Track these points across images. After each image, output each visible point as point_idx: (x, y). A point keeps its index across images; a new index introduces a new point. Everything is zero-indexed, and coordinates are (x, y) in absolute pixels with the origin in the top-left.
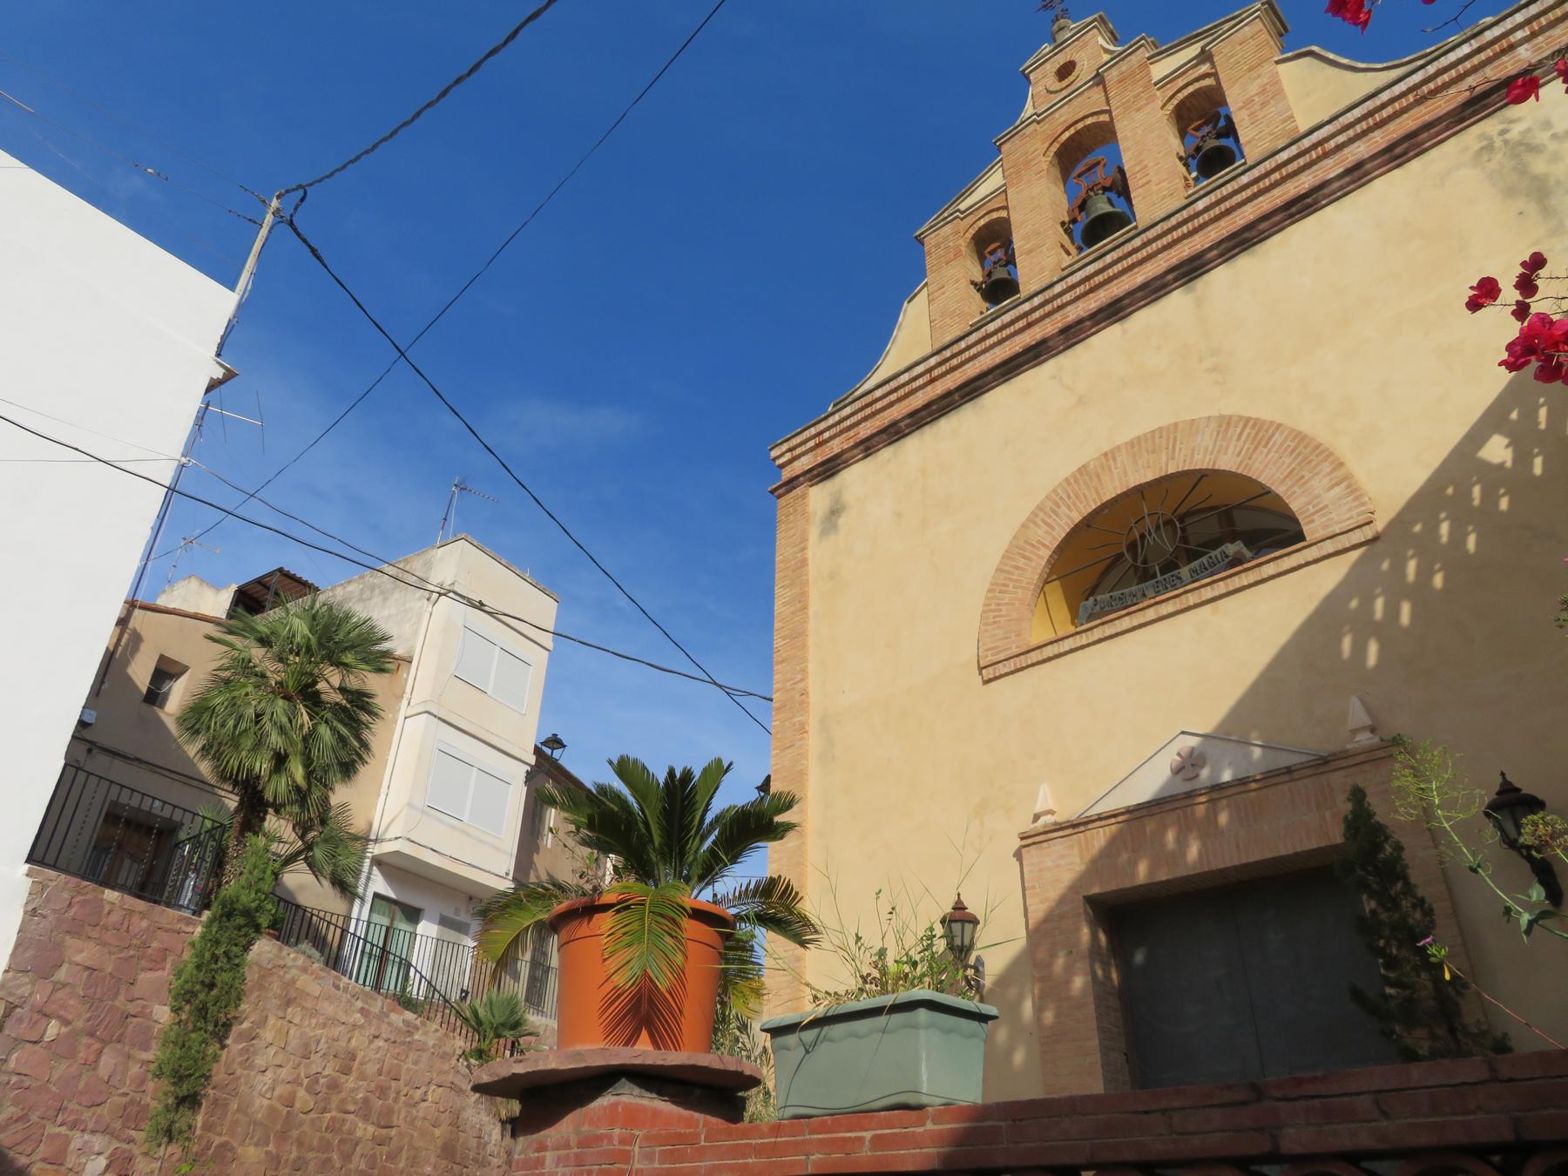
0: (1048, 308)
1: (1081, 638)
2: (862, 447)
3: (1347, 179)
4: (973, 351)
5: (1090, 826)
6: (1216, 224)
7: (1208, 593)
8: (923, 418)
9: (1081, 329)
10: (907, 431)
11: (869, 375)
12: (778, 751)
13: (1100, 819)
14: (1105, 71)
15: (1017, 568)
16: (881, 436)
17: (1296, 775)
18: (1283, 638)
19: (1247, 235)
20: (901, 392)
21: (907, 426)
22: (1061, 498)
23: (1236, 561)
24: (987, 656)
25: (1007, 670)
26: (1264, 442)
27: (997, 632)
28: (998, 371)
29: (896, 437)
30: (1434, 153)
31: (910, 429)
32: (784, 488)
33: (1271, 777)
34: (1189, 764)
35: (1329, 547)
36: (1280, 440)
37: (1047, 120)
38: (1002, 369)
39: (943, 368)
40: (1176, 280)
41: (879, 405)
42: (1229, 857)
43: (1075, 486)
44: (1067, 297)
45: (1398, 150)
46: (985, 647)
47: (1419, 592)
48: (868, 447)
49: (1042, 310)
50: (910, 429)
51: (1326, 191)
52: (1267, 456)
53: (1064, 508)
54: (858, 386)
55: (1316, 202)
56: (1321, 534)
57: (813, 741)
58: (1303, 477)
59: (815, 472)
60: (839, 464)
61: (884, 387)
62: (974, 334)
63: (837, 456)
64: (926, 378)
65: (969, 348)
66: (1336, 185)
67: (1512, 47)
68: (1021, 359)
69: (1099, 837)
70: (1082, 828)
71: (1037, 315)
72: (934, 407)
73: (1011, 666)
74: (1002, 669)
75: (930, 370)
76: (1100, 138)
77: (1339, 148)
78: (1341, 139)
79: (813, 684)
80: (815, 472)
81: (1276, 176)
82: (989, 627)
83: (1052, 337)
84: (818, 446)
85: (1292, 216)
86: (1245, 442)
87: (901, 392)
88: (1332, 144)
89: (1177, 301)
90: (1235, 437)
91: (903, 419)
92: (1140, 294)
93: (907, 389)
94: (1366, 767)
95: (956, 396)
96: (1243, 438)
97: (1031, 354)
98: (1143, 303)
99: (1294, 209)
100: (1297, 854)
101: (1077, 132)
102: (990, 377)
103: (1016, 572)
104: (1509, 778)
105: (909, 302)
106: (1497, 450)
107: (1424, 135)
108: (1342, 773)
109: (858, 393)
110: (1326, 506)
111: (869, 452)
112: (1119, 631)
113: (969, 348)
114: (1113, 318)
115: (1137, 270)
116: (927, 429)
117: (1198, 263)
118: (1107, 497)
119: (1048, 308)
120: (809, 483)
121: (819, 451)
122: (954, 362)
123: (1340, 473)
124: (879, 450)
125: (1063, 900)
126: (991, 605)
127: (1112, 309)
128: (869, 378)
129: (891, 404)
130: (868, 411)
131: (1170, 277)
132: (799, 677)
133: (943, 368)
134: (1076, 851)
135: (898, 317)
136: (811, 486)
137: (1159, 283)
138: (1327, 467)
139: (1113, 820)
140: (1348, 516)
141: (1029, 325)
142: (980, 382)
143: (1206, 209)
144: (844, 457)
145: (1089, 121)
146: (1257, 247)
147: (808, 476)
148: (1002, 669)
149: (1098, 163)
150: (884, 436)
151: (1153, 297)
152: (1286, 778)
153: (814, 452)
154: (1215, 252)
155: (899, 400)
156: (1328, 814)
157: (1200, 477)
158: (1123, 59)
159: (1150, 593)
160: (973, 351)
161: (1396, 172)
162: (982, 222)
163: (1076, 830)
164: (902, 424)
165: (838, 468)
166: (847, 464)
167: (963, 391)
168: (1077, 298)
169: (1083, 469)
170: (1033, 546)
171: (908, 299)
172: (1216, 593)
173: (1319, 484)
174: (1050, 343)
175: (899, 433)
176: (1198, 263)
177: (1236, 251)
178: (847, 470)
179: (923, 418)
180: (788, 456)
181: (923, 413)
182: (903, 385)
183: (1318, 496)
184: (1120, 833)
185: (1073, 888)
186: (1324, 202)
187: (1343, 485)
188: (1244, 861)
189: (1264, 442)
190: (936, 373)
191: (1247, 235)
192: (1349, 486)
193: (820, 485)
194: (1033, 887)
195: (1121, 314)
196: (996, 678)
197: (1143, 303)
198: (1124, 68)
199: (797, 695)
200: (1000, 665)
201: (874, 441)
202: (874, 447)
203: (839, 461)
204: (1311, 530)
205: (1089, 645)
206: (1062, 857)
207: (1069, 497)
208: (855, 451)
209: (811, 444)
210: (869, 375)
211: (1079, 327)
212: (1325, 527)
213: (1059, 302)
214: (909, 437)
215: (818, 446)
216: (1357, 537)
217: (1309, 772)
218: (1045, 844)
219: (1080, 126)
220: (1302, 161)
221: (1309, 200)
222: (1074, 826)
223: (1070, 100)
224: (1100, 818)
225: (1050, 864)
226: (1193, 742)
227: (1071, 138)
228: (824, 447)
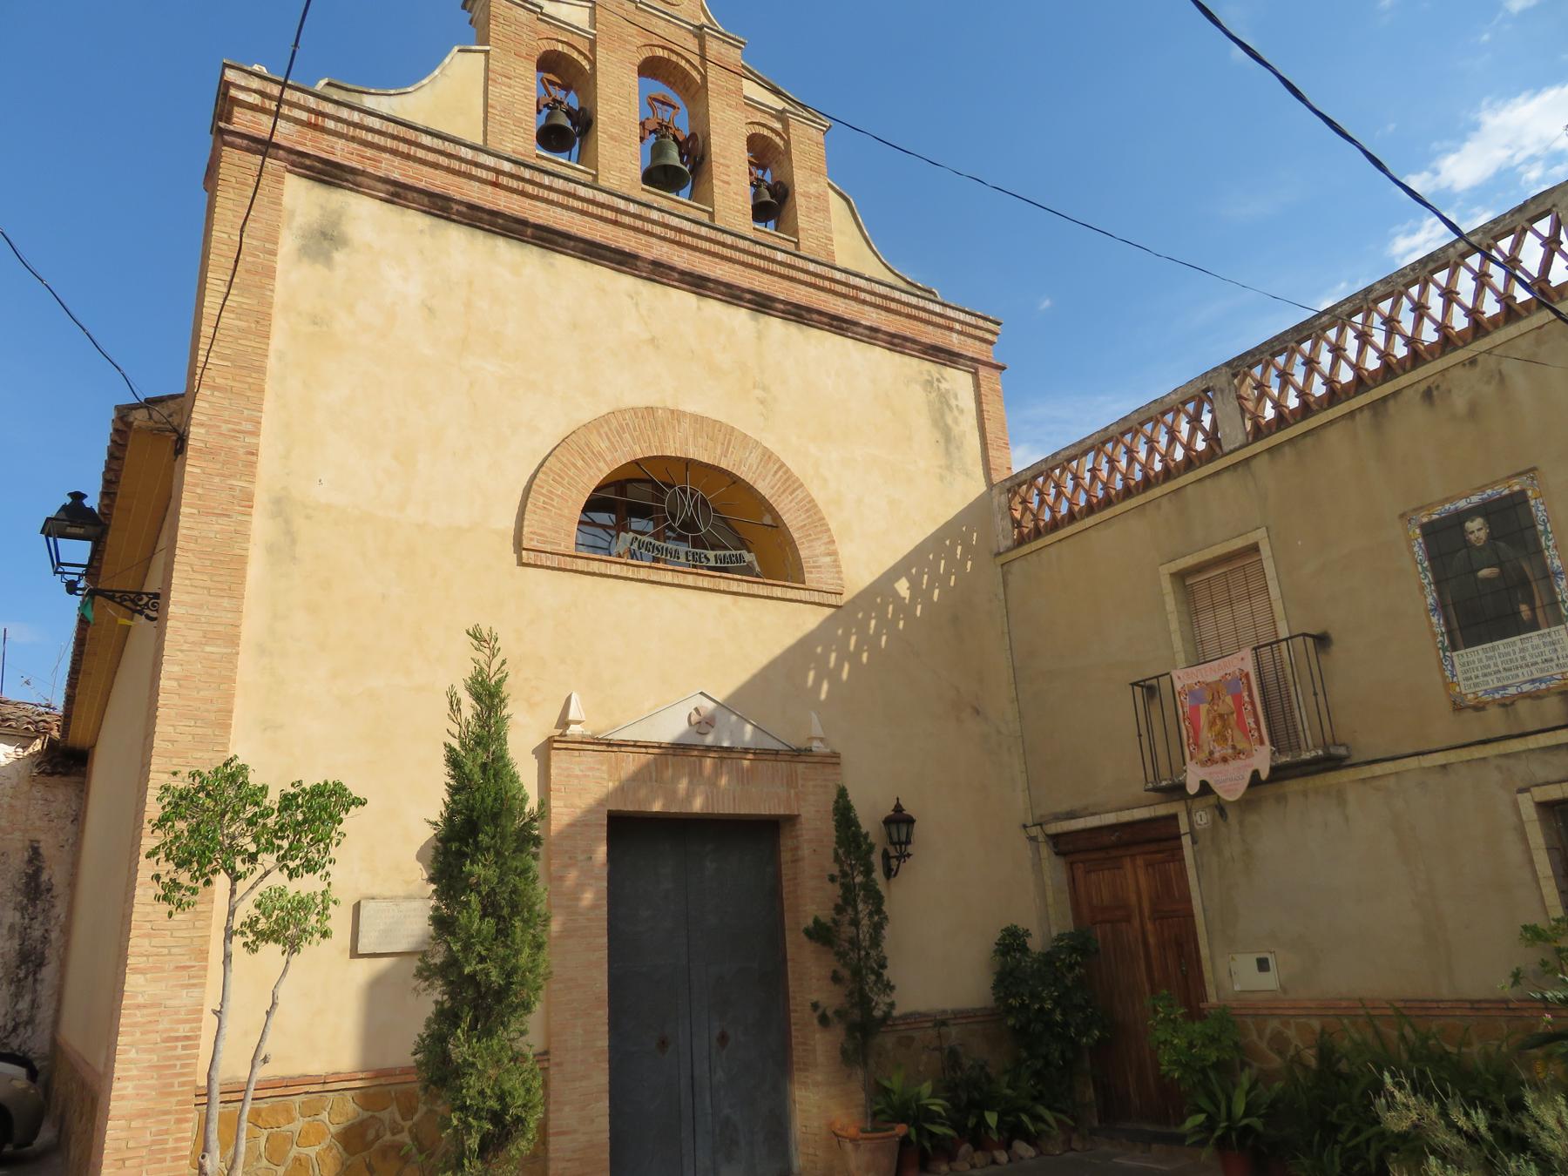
0: (639, 223)
1: (629, 570)
2: (392, 189)
3: (867, 332)
4: (554, 196)
5: (623, 749)
6: (780, 280)
7: (734, 587)
8: (480, 220)
9: (667, 274)
10: (454, 217)
11: (392, 92)
12: (195, 511)
13: (634, 746)
14: (708, 33)
15: (574, 465)
16: (422, 196)
17: (779, 758)
18: (777, 650)
19: (804, 313)
20: (455, 165)
21: (459, 213)
22: (627, 424)
23: (748, 570)
24: (532, 539)
25: (549, 564)
26: (790, 490)
27: (547, 520)
28: (582, 245)
29: (439, 213)
30: (906, 359)
31: (461, 219)
32: (246, 142)
33: (760, 754)
34: (704, 723)
35: (816, 597)
36: (800, 497)
37: (643, 14)
38: (587, 247)
39: (514, 184)
40: (749, 301)
41: (421, 153)
42: (726, 807)
43: (642, 422)
44: (657, 230)
45: (896, 341)
46: (531, 529)
47: (854, 658)
48: (399, 194)
49: (632, 219)
50: (461, 219)
51: (855, 329)
52: (791, 502)
53: (627, 435)
54: (373, 91)
55: (847, 330)
56: (814, 585)
57: (260, 526)
58: (810, 535)
59: (308, 162)
60: (347, 181)
61: (435, 140)
62: (561, 181)
63: (353, 171)
64: (491, 176)
65: (550, 188)
66: (861, 330)
67: (951, 329)
68: (608, 254)
69: (631, 763)
70: (615, 749)
71: (626, 220)
72: (500, 221)
73: (555, 561)
74: (545, 559)
75: (498, 172)
76: (671, 79)
77: (864, 302)
78: (868, 298)
79: (268, 443)
80: (308, 162)
81: (827, 284)
82: (538, 511)
83: (644, 260)
84: (309, 125)
85: (831, 326)
86: (778, 481)
87: (455, 165)
88: (863, 295)
89: (740, 317)
90: (772, 472)
91: (460, 203)
92: (722, 288)
93: (464, 167)
94: (818, 766)
95: (529, 231)
96: (778, 476)
97: (617, 257)
98: (719, 296)
99: (835, 323)
100: (770, 815)
101: (669, 60)
102: (572, 243)
103: (573, 470)
104: (901, 802)
105: (459, 51)
106: (902, 587)
107: (909, 344)
108: (804, 765)
109: (369, 102)
110: (820, 567)
111: (396, 200)
112: (662, 580)
113: (550, 188)
114: (694, 289)
115: (717, 260)
116: (479, 233)
117: (769, 303)
118: (670, 452)
119: (639, 223)
120: (289, 167)
121: (310, 133)
122: (530, 189)
123: (832, 548)
124: (408, 207)
125: (590, 811)
126: (543, 488)
127: (699, 281)
128: (391, 95)
129: (435, 166)
130: (403, 148)
131: (748, 296)
132: (248, 426)
133: (514, 184)
134: (604, 768)
135: (444, 58)
136: (290, 171)
137: (738, 293)
138: (825, 539)
139: (644, 750)
140: (832, 581)
141: (615, 223)
142: (560, 240)
143: (781, 263)
144: (359, 179)
145: (683, 63)
146: (804, 326)
147: (294, 157)
148: (545, 559)
149: (674, 107)
150: (426, 200)
151: (729, 299)
152: (773, 757)
153: (298, 127)
154: (781, 306)
155: (448, 170)
156: (792, 792)
157: (735, 481)
158: (724, 41)
159: (683, 560)
160: (554, 196)
161: (887, 351)
162: (560, 47)
163: (610, 749)
164: (455, 207)
165: (345, 184)
166: (356, 188)
167: (539, 233)
168: (664, 239)
169: (651, 410)
170: (593, 453)
171: (462, 47)
172: (740, 590)
173: (820, 548)
174: (639, 263)
175: (444, 211)
176: (769, 303)
177: (792, 317)
178: (353, 194)
179: (480, 220)
180: (254, 99)
181: (486, 217)
182: (461, 160)
183: (817, 556)
184: (648, 765)
185: (601, 803)
186: (850, 334)
187: (833, 558)
188: (737, 812)
189: (790, 490)
190: (504, 180)
191: (804, 313)
192: (835, 561)
193: (308, 183)
194: (559, 790)
195: (701, 291)
196: (535, 566)
197: (719, 296)
198: (723, 51)
199: (241, 451)
200: (543, 555)
201: (410, 195)
202: (406, 199)
203: (349, 177)
204: (811, 578)
205: (632, 579)
206: (591, 769)
207: (635, 430)
208: (379, 185)
209: (304, 116)
210: (392, 92)
211: (668, 271)
212: (818, 582)
213: (648, 227)
214: (453, 225)
215: (309, 125)
216: (833, 600)
217: (788, 758)
218: (576, 753)
219: (674, 58)
220: (844, 290)
221: (845, 325)
222: (609, 745)
223: (669, 21)
224: (635, 745)
225: (577, 772)
226: (710, 705)
227: (661, 58)
228: (318, 134)
